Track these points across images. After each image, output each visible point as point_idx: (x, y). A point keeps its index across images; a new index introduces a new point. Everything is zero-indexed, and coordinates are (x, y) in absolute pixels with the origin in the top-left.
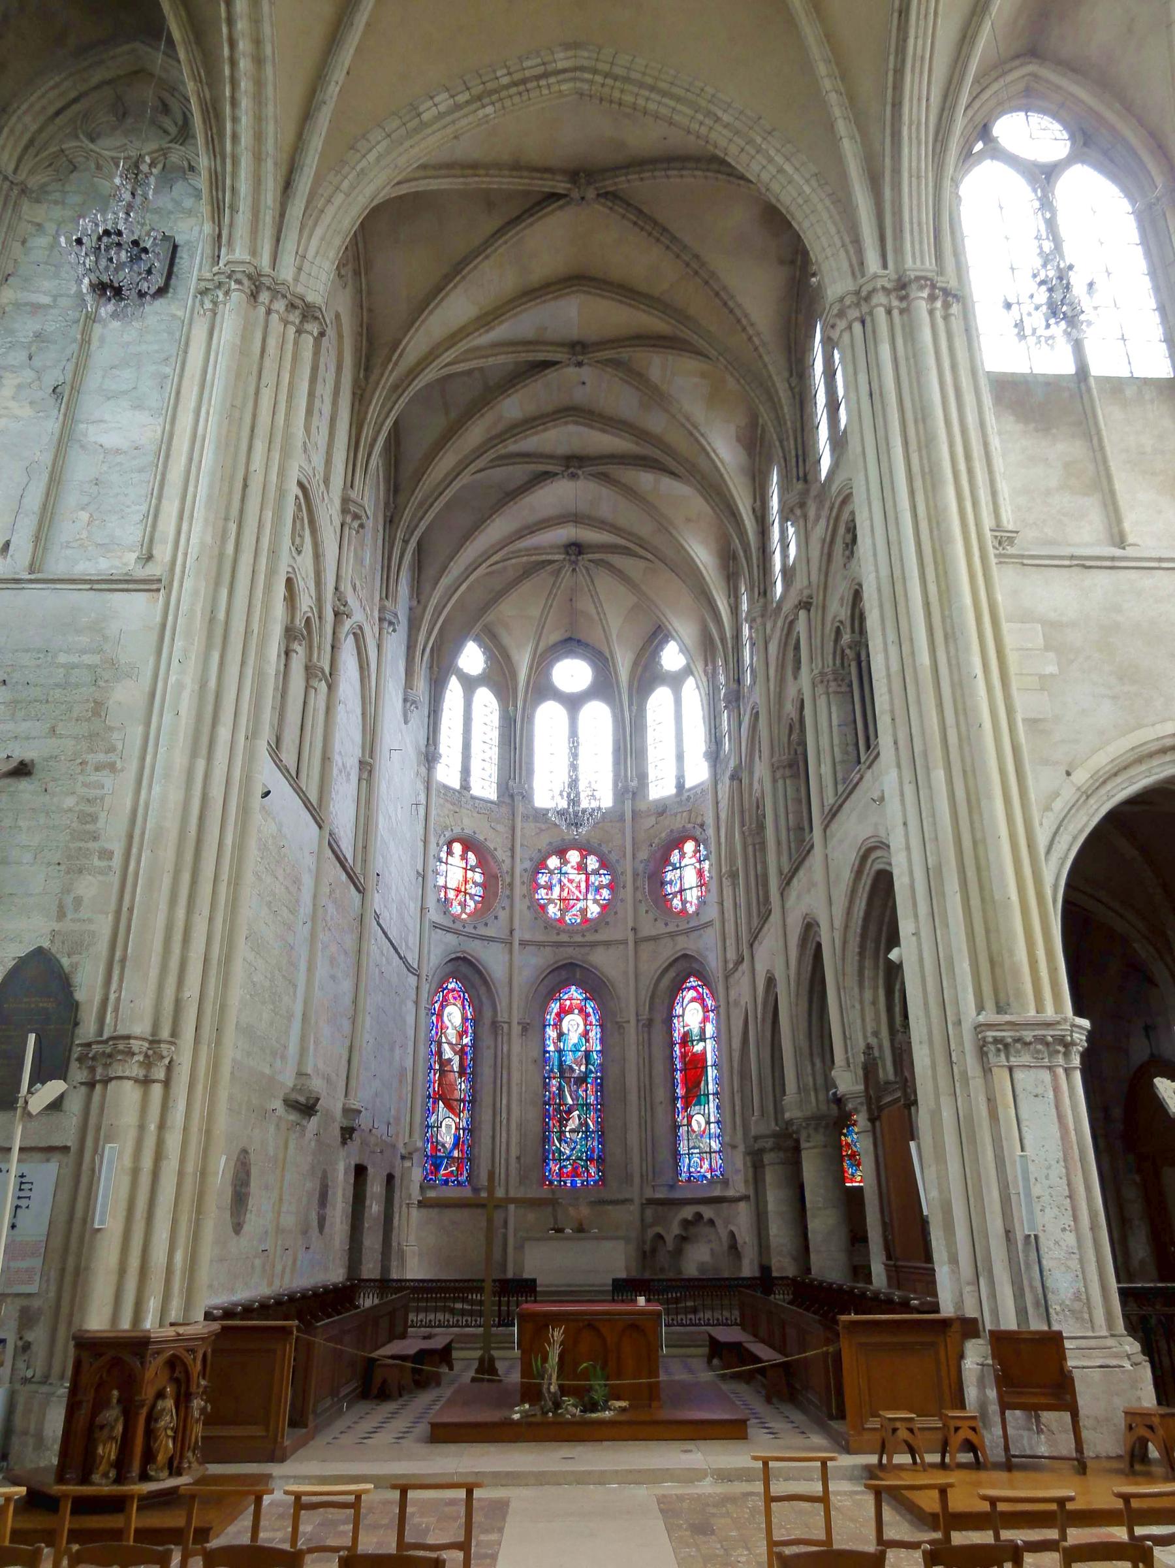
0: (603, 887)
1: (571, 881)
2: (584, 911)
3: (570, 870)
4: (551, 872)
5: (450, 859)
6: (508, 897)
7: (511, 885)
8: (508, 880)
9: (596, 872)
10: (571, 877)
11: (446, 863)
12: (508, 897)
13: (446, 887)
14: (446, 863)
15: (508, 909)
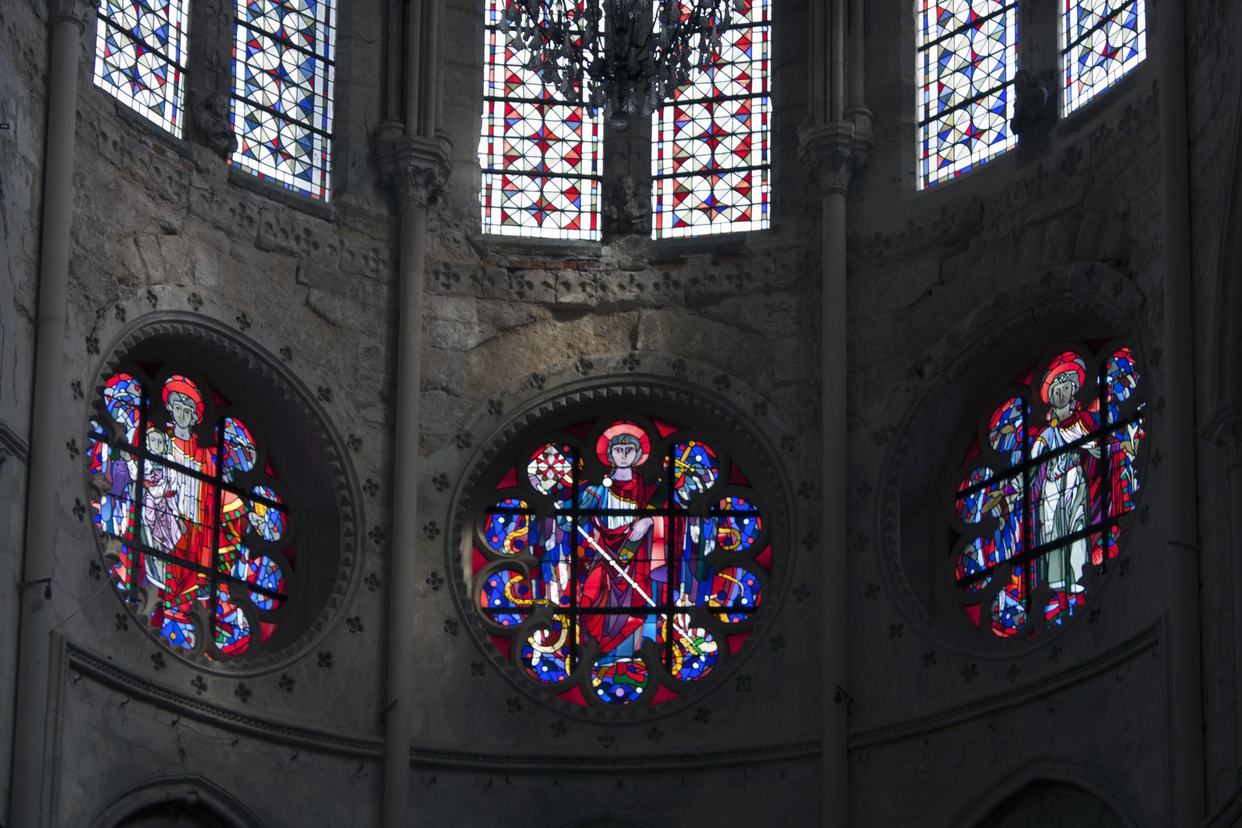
0: (725, 559)
1: (614, 540)
2: (665, 647)
3: (614, 502)
4: (540, 507)
5: (154, 442)
6: (372, 580)
7: (387, 536)
8: (373, 515)
9: (706, 507)
10: (614, 523)
11: (140, 452)
12: (372, 580)
13: (134, 541)
14: (140, 452)
15: (371, 620)
